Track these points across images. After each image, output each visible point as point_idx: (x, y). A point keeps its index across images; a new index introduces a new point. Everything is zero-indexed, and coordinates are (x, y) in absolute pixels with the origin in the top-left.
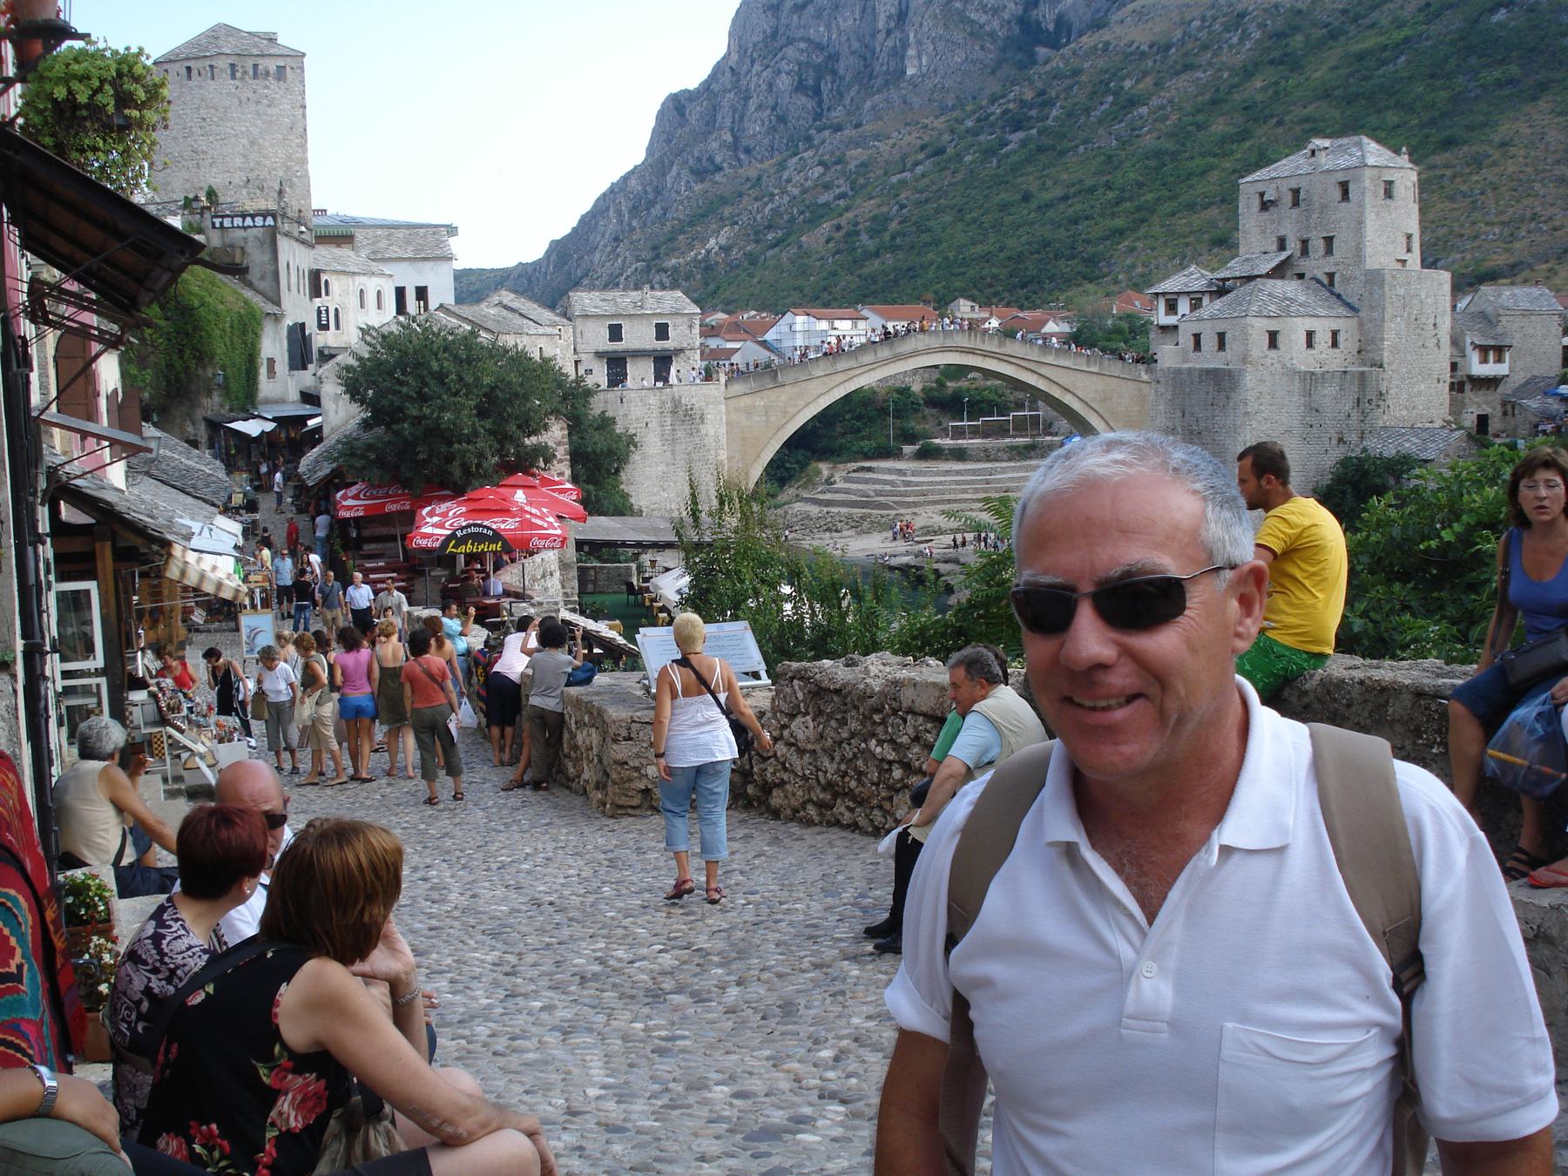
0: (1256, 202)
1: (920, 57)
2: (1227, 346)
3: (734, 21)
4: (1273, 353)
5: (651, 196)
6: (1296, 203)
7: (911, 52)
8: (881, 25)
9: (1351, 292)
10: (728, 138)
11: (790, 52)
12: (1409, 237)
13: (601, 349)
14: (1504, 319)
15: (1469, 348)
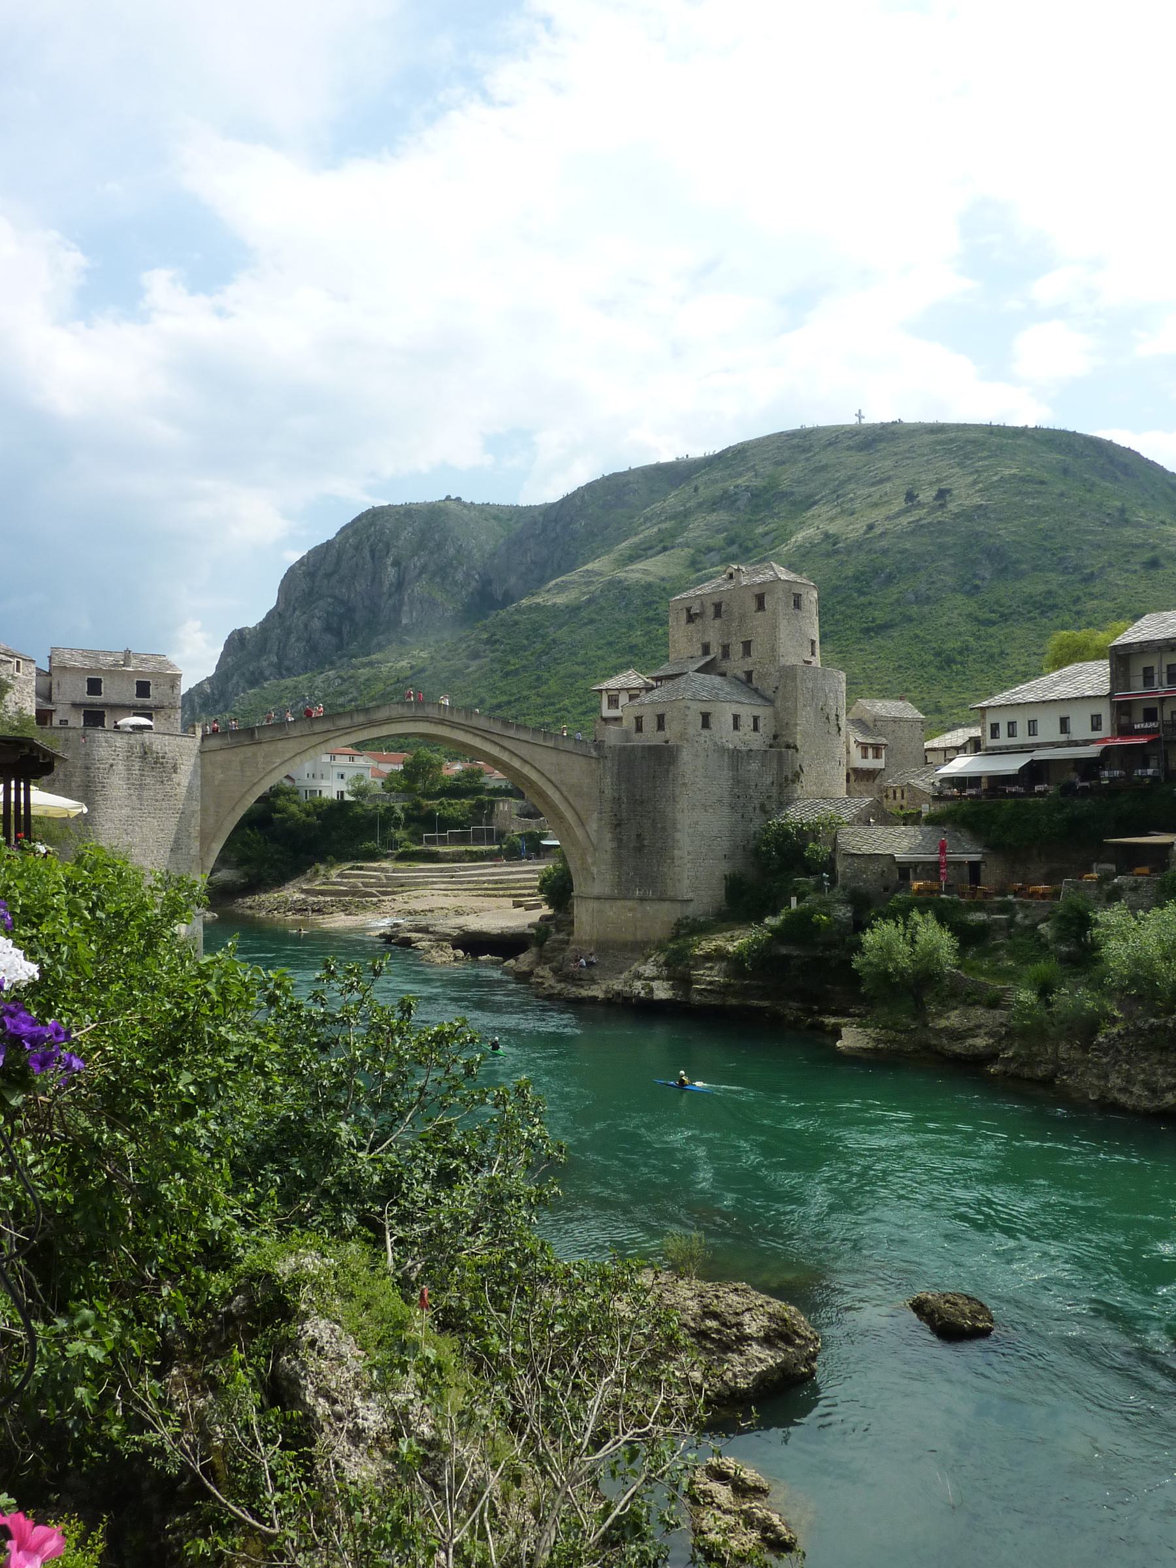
0: (684, 616)
1: (411, 613)
2: (666, 726)
3: (282, 581)
4: (705, 732)
5: (216, 697)
6: (718, 613)
7: (405, 608)
8: (385, 589)
9: (767, 686)
10: (275, 659)
11: (321, 603)
12: (813, 642)
13: (78, 700)
14: (879, 724)
15: (853, 746)
